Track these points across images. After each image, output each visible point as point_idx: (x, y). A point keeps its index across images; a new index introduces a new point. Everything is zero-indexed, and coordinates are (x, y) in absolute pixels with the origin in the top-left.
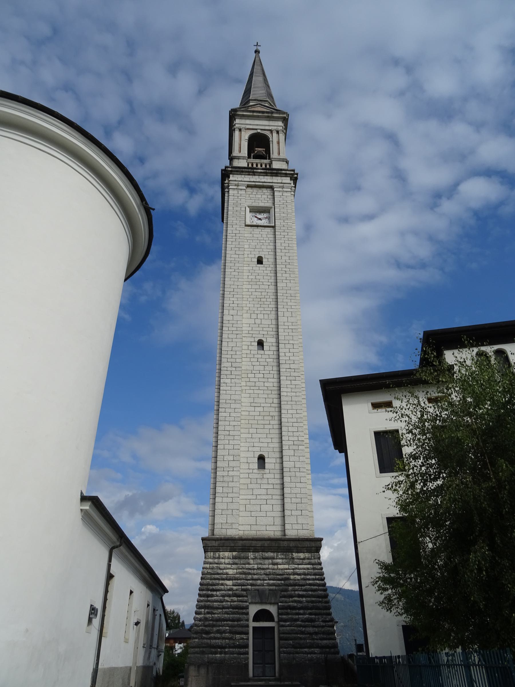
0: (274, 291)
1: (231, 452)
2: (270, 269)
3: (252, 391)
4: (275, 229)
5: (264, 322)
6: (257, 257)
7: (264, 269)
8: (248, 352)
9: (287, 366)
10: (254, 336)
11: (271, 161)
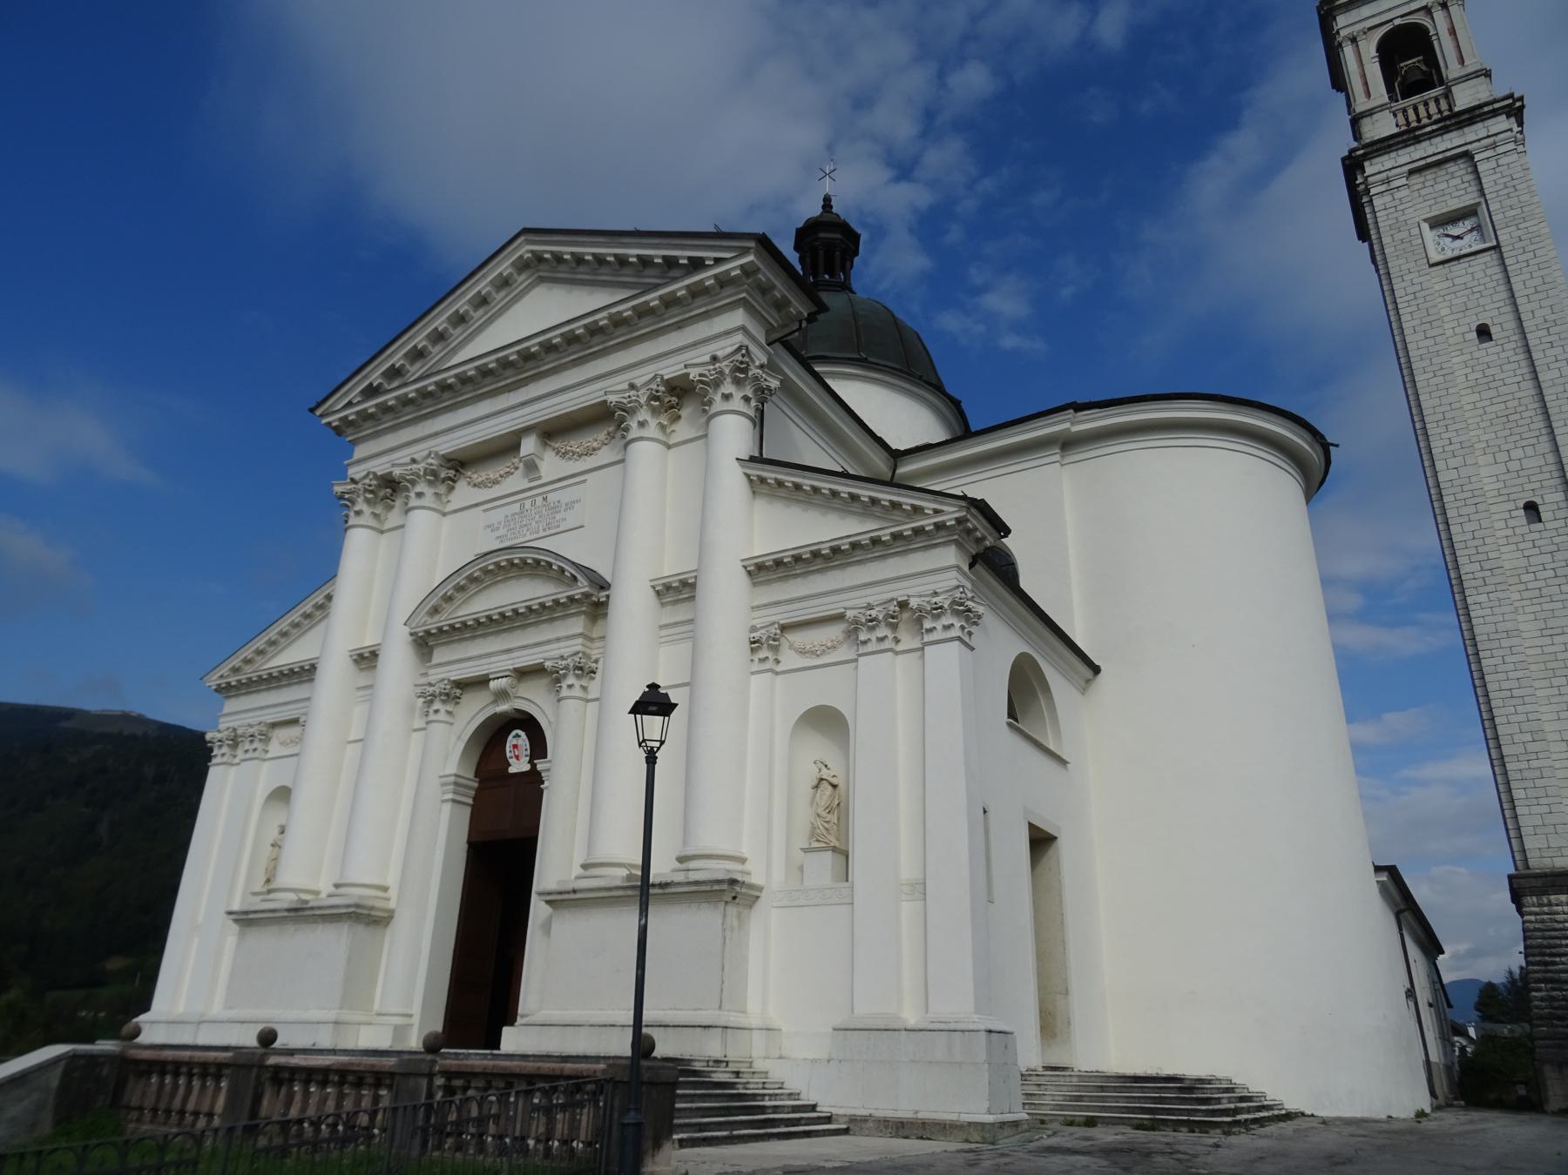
0: (1533, 392)
1: (1525, 727)
2: (1513, 345)
3: (1538, 608)
4: (1501, 254)
5: (1526, 463)
6: (1475, 328)
8: (1510, 532)
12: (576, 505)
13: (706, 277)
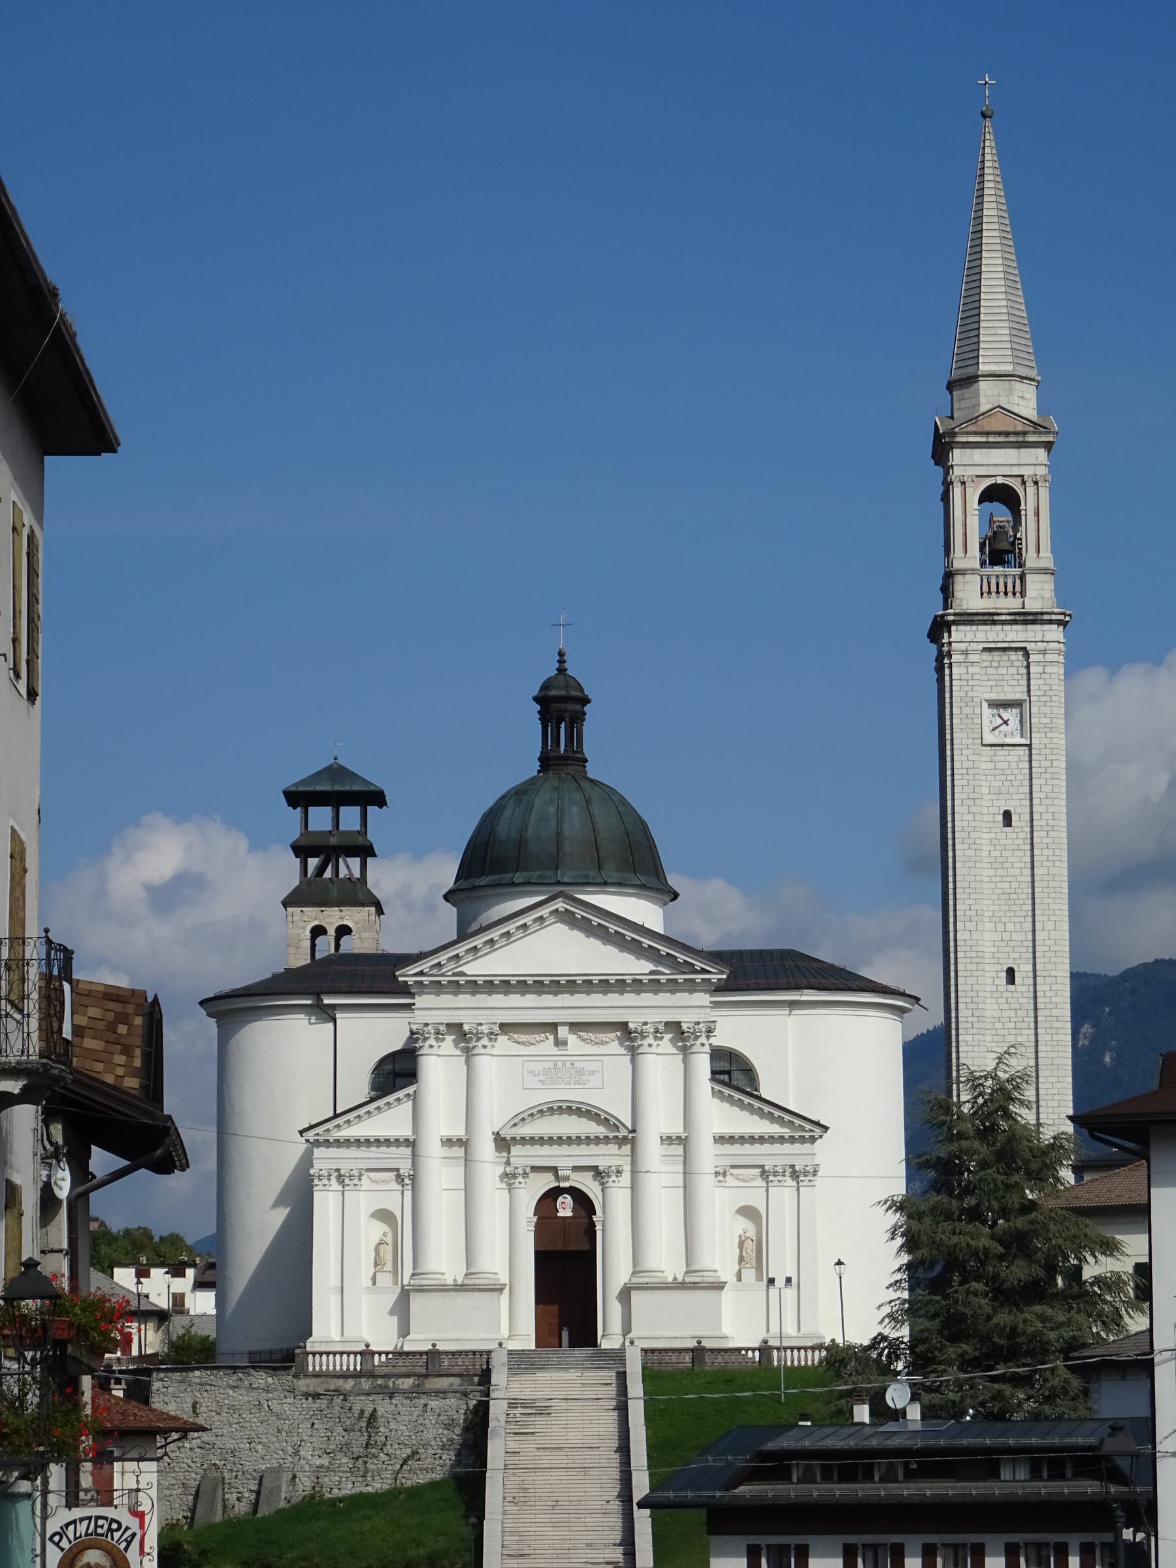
5: (1015, 937)
7: (1014, 836)
8: (994, 988)
9: (1047, 1013)
10: (1001, 961)
11: (1023, 571)
12: (596, 1074)
13: (698, 977)
